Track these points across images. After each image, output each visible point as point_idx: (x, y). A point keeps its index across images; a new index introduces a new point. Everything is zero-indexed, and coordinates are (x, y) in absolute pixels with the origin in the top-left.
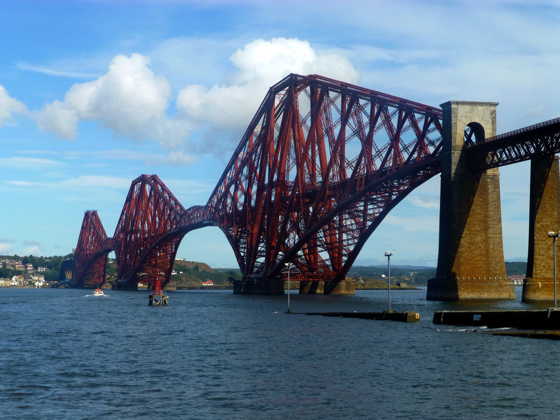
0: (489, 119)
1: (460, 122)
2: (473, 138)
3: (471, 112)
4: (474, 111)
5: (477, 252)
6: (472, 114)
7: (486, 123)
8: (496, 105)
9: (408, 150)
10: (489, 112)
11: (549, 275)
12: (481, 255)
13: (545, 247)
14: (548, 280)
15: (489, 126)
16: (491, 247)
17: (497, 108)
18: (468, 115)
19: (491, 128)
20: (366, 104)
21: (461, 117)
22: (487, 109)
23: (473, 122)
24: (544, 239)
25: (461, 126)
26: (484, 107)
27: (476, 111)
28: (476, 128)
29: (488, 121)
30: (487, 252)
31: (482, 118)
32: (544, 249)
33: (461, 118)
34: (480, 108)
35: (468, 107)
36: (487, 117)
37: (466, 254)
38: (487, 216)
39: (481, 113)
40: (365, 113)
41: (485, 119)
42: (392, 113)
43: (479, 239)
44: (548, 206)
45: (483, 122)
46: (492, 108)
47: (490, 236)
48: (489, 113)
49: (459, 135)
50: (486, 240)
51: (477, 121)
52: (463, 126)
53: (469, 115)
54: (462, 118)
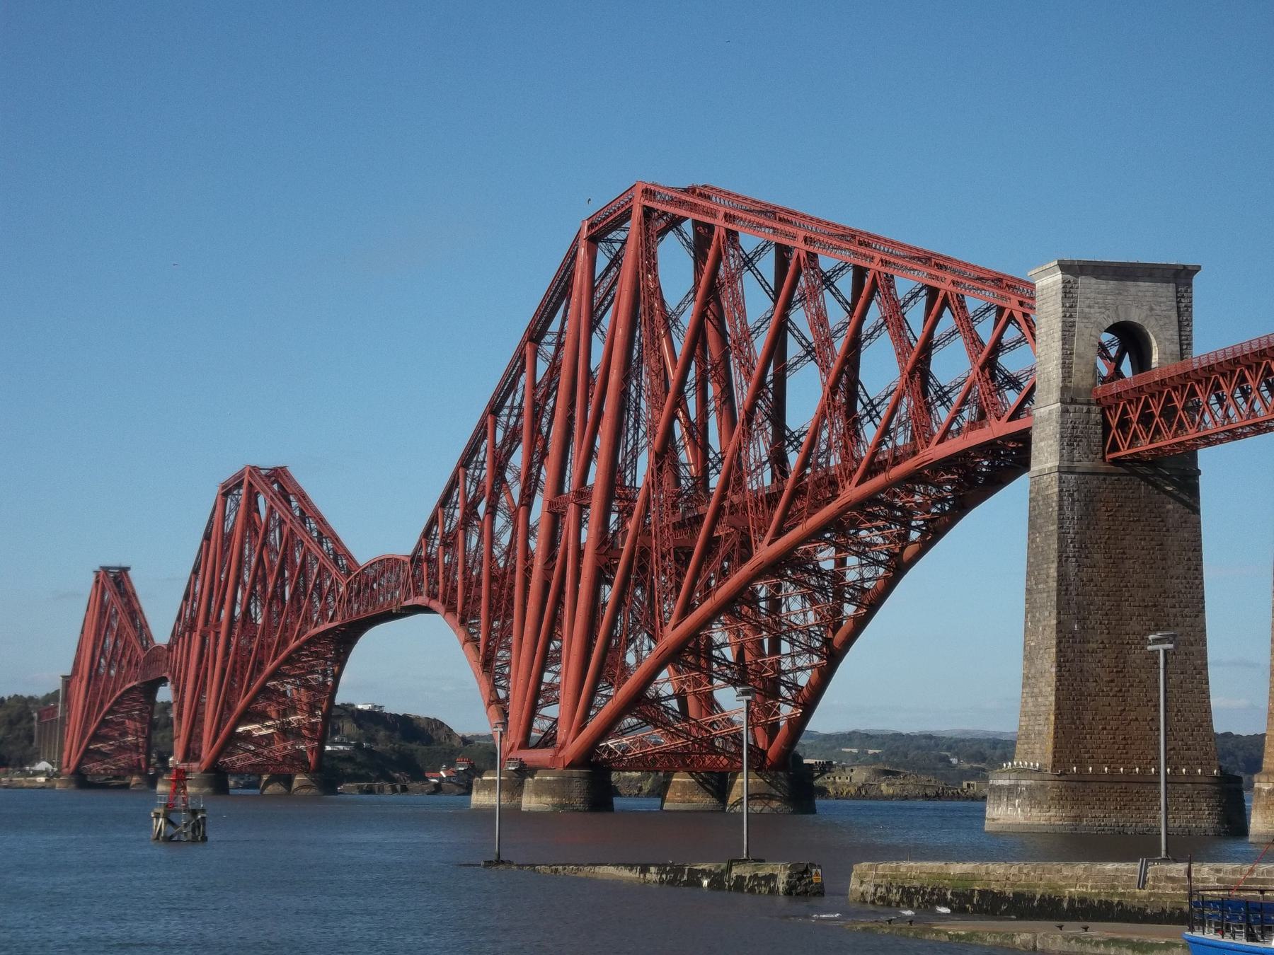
1: (1086, 321)
2: (1126, 367)
3: (1120, 294)
7: (1161, 323)
9: (949, 400)
15: (1171, 332)
17: (1196, 280)
18: (1110, 299)
20: (841, 269)
21: (1089, 307)
23: (1122, 319)
25: (1087, 332)
29: (1169, 317)
31: (1151, 309)
33: (1087, 310)
39: (1149, 294)
40: (836, 294)
41: (1159, 313)
42: (909, 296)
45: (1153, 322)
49: (1082, 358)
51: (1135, 316)
52: (1093, 333)
53: (1111, 302)
54: (1092, 311)
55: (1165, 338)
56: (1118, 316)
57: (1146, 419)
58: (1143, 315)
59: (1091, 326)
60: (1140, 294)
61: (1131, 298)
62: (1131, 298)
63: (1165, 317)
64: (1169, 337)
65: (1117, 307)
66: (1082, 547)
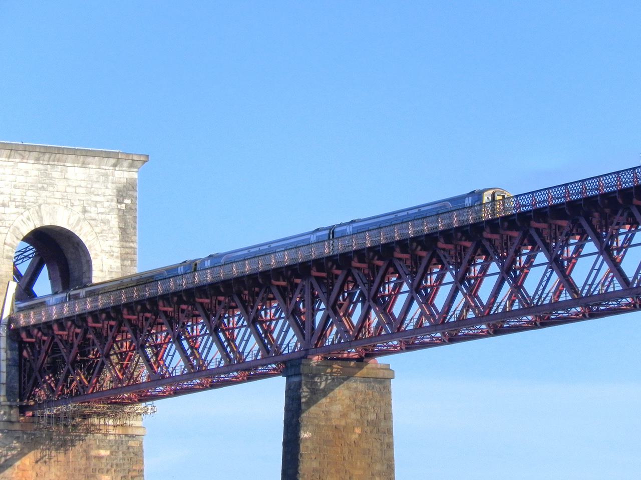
0: (108, 217)
3: (43, 188)
4: (52, 185)
6: (44, 194)
7: (97, 230)
15: (110, 243)
18: (31, 196)
19: (117, 251)
22: (102, 179)
27: (61, 185)
31: (85, 211)
36: (101, 210)
39: (79, 190)
41: (94, 215)
46: (123, 175)
48: (109, 192)
52: (8, 241)
53: (32, 199)
54: (7, 210)
55: (102, 251)
56: (41, 218)
58: (73, 220)
59: (6, 231)
60: (69, 190)
61: (58, 195)
62: (58, 195)
63: (103, 222)
64: (108, 249)
65: (40, 206)
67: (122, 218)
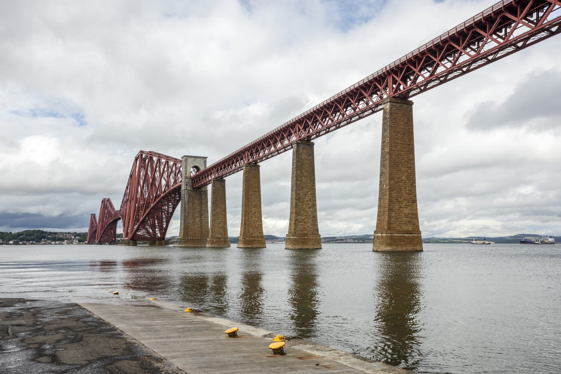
5: (196, 226)
8: (206, 158)
10: (203, 161)
11: (219, 236)
12: (198, 227)
13: (217, 222)
14: (219, 238)
16: (203, 224)
17: (207, 159)
18: (193, 162)
24: (217, 219)
26: (201, 159)
28: (197, 168)
30: (201, 226)
32: (217, 224)
34: (199, 159)
35: (193, 159)
37: (191, 227)
38: (201, 210)
43: (197, 220)
44: (219, 203)
46: (205, 160)
47: (203, 218)
50: (201, 221)
57: (197, 181)
66: (188, 202)
67: (205, 165)
